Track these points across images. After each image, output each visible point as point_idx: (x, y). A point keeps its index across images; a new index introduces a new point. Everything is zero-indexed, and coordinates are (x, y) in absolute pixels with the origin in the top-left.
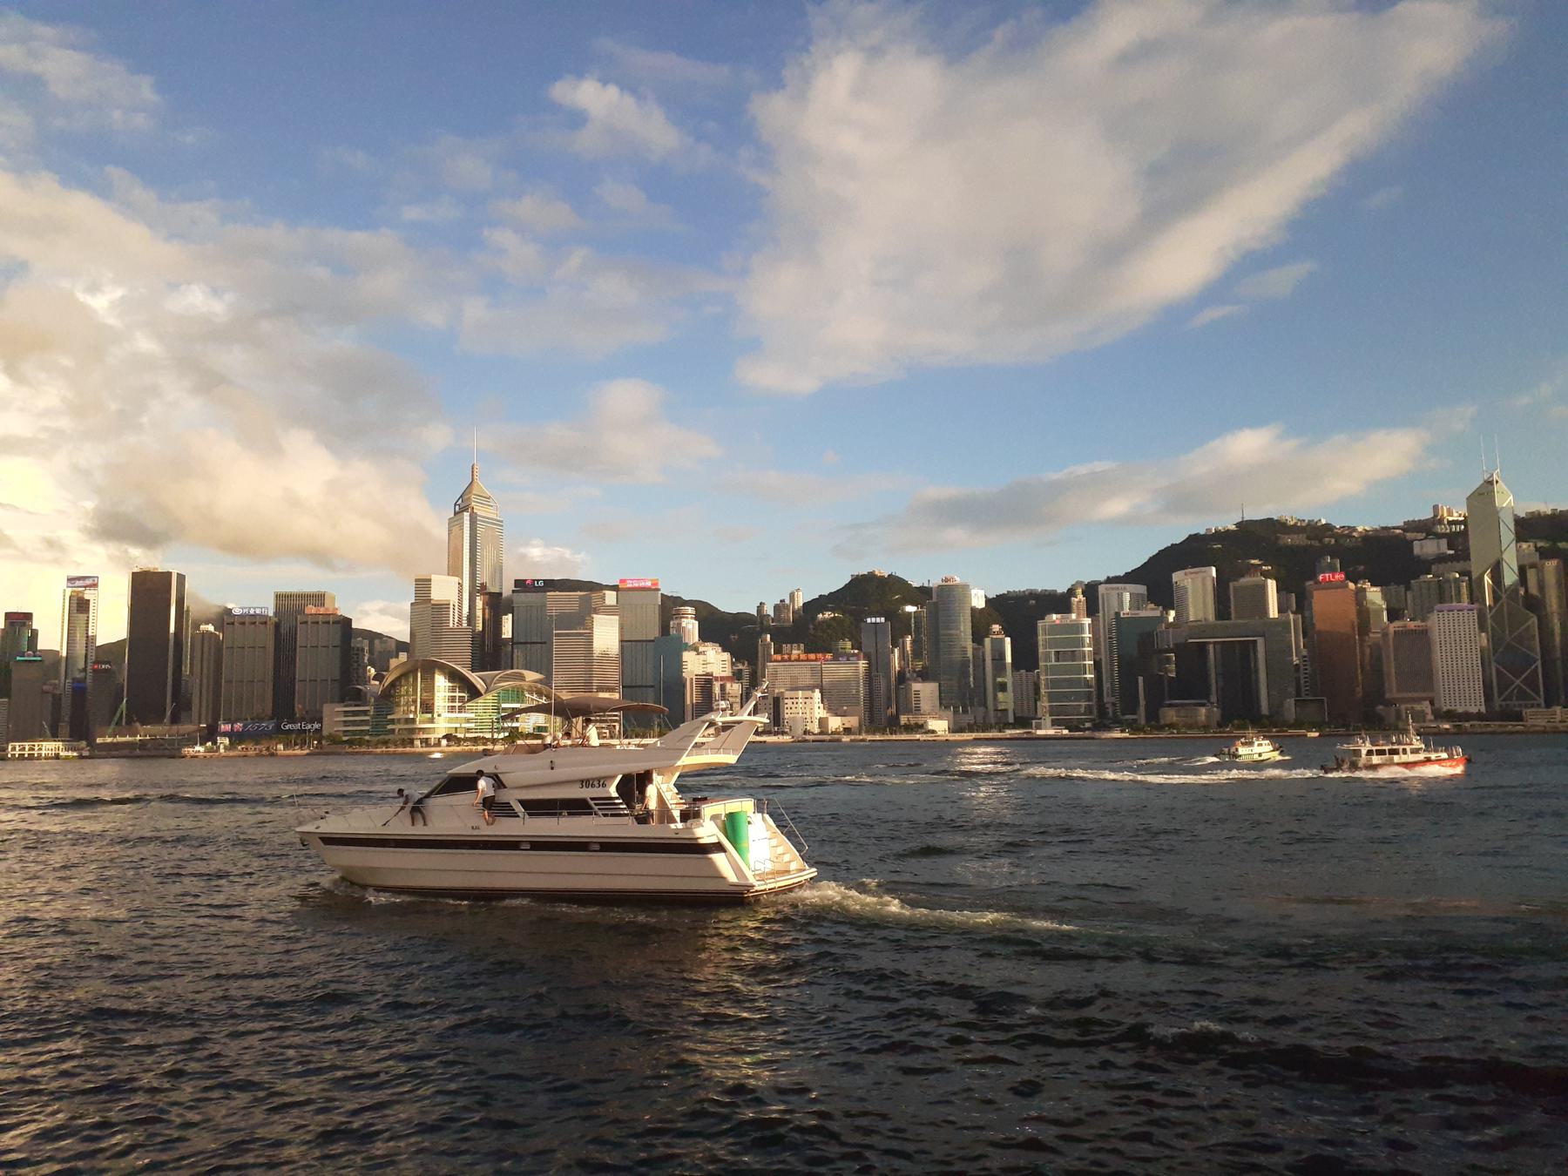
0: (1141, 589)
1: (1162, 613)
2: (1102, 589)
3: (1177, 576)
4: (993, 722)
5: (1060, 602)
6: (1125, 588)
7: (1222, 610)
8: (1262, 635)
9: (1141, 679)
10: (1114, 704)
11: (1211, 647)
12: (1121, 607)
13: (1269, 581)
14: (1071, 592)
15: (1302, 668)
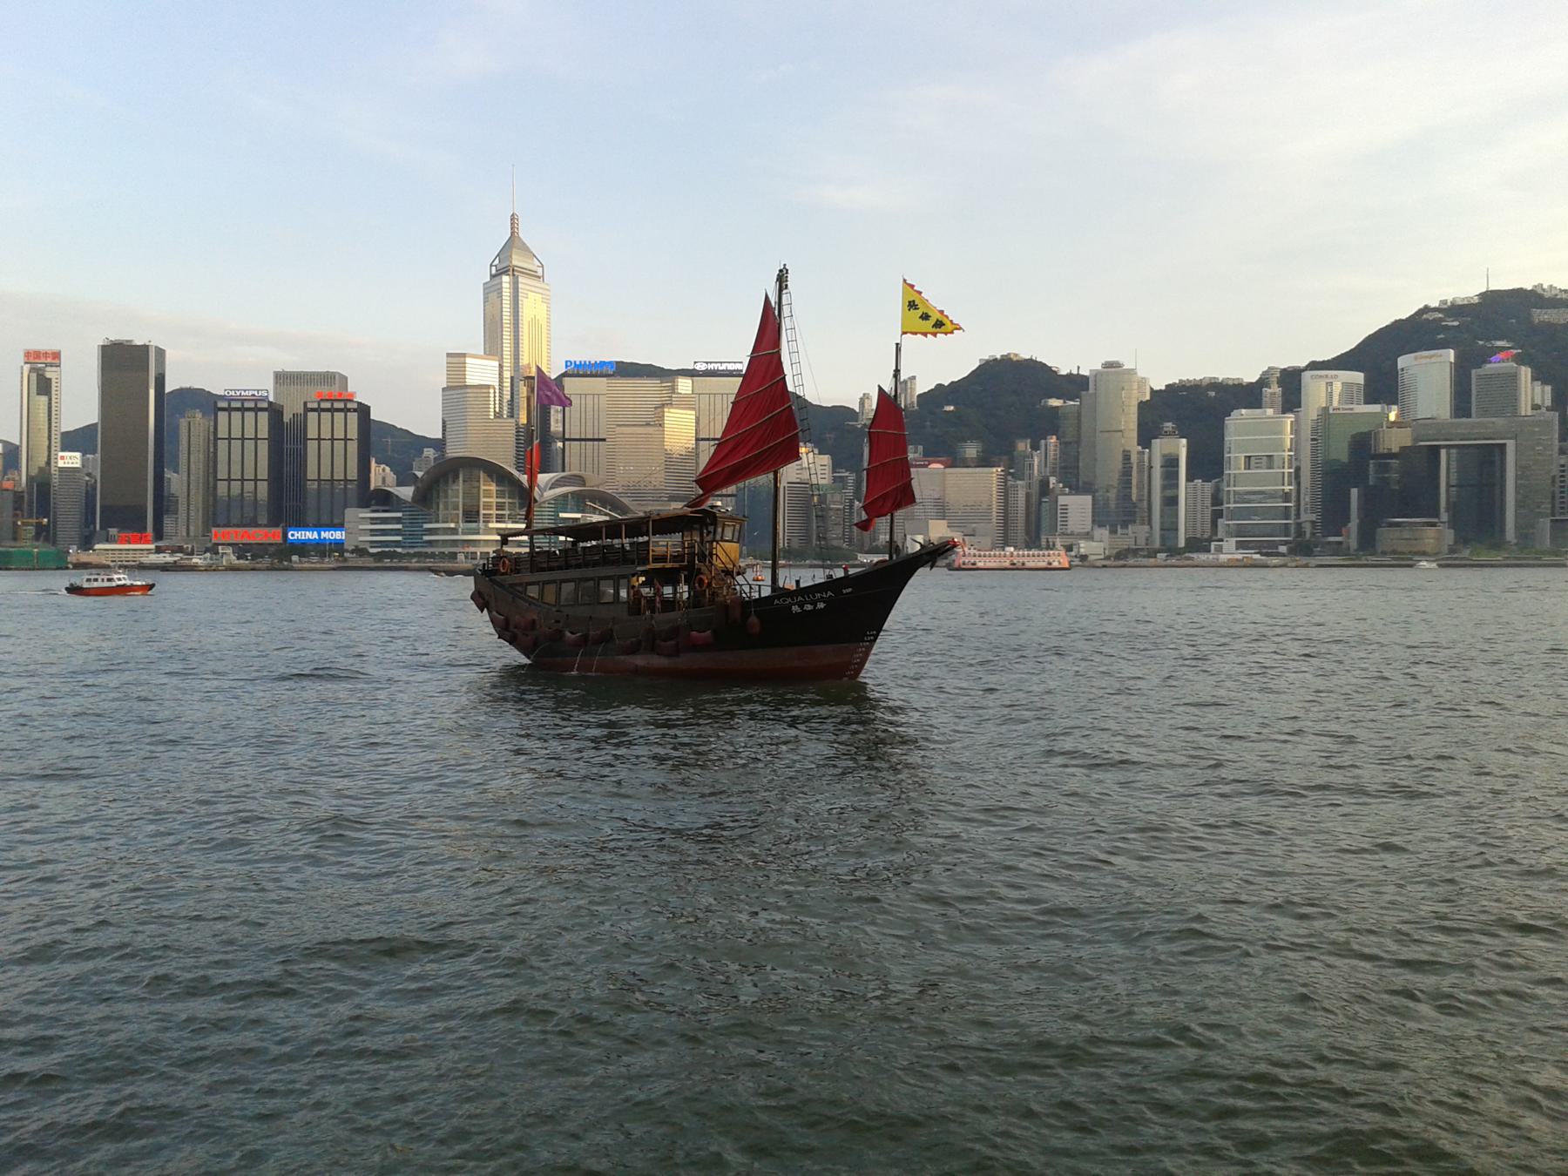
0: (1358, 377)
1: (1383, 409)
2: (1306, 375)
3: (1403, 361)
4: (1157, 544)
5: (1249, 395)
6: (1336, 376)
7: (1461, 404)
8: (1515, 438)
9: (1354, 492)
10: (1313, 522)
11: (1443, 452)
12: (1330, 395)
13: (1523, 368)
14: (1263, 382)
15: (1558, 480)
